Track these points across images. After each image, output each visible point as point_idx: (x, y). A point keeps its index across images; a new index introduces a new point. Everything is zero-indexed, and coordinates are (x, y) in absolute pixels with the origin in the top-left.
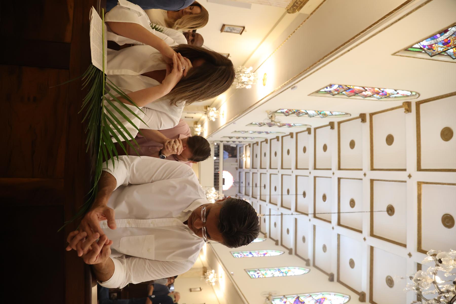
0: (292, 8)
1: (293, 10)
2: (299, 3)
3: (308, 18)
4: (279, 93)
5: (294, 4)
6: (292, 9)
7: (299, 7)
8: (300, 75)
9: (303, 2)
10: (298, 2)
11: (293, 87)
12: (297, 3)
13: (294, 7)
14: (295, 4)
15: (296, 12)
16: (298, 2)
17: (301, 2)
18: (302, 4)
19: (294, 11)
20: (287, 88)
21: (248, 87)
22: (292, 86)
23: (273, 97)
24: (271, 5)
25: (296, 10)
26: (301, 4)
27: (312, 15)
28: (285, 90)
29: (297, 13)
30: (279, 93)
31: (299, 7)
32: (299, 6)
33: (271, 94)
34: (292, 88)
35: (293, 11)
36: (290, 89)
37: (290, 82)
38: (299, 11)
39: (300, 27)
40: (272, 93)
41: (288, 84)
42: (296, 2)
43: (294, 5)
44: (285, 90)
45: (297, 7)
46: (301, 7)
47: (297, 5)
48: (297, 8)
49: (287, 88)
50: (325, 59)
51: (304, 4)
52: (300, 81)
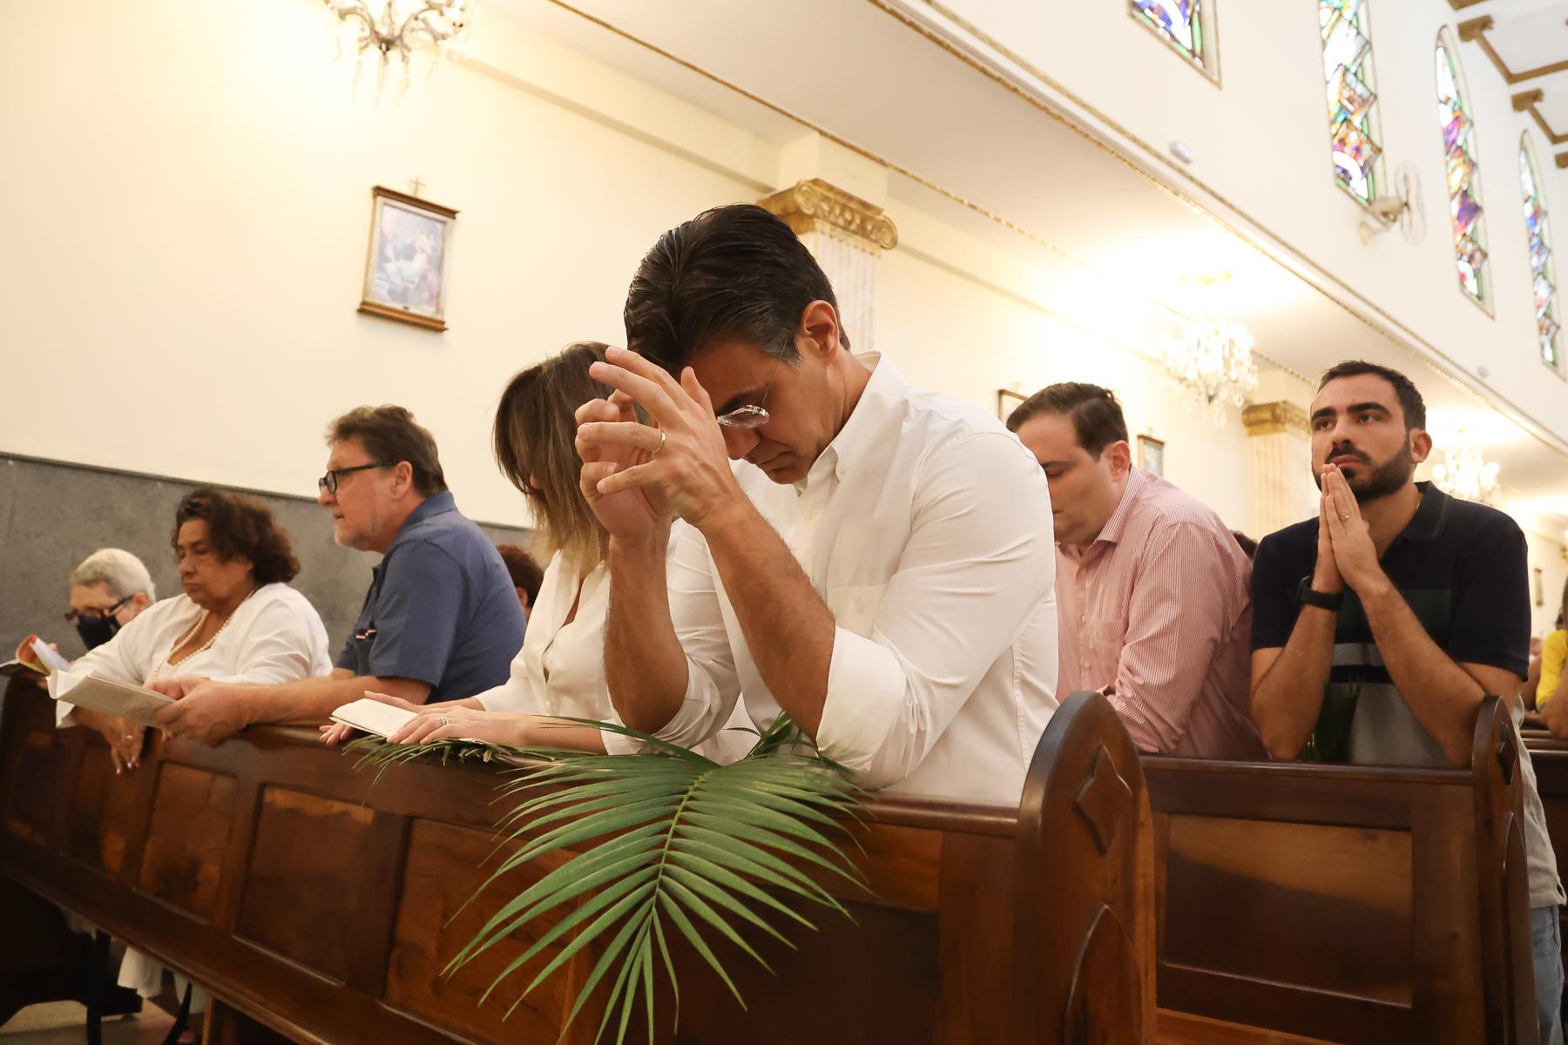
0: (873, 237)
1: (880, 229)
2: (848, 216)
3: (903, 172)
4: (1231, 206)
5: (855, 232)
6: (879, 235)
7: (868, 213)
8: (1103, 142)
9: (842, 201)
10: (846, 220)
11: (1179, 160)
12: (850, 222)
13: (869, 227)
14: (853, 227)
15: (885, 217)
16: (846, 220)
17: (844, 208)
18: (853, 205)
19: (887, 226)
20: (1192, 179)
21: (1246, 343)
22: (1170, 164)
23: (1259, 226)
24: (871, 310)
25: (879, 221)
26: (851, 210)
27: (887, 160)
28: (1203, 187)
29: (891, 210)
30: (1231, 206)
31: (868, 213)
32: (858, 212)
33: (1246, 239)
34: (1187, 161)
35: (884, 229)
36: (1189, 169)
37: (1155, 177)
38: (882, 210)
39: (946, 189)
40: (1238, 234)
41: (1167, 184)
42: (845, 228)
43: (862, 231)
44: (1203, 187)
45: (863, 221)
46: (864, 204)
47: (858, 221)
48: (871, 218)
49: (1192, 179)
50: (996, 74)
51: (850, 198)
52: (1135, 140)
